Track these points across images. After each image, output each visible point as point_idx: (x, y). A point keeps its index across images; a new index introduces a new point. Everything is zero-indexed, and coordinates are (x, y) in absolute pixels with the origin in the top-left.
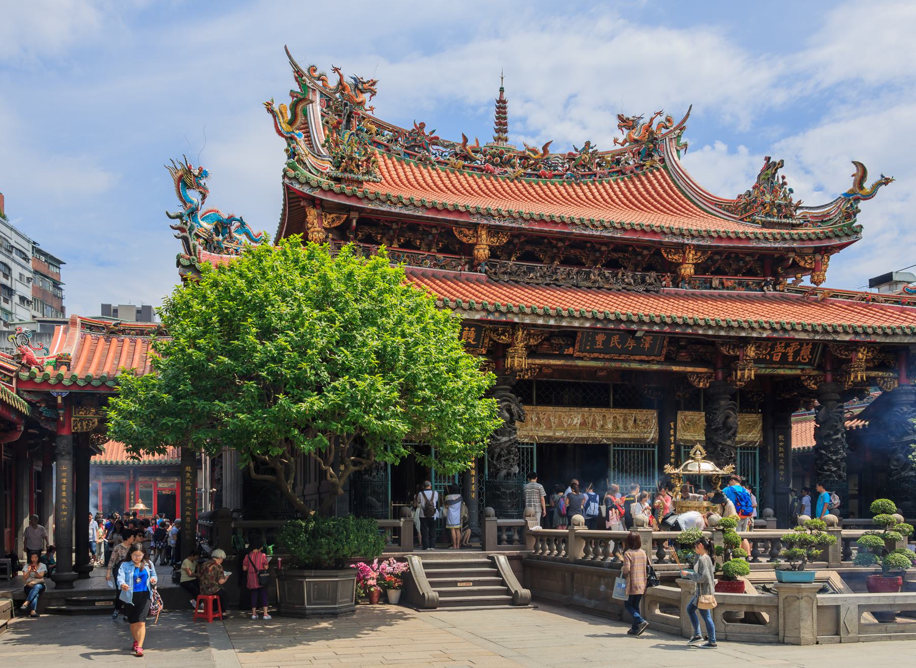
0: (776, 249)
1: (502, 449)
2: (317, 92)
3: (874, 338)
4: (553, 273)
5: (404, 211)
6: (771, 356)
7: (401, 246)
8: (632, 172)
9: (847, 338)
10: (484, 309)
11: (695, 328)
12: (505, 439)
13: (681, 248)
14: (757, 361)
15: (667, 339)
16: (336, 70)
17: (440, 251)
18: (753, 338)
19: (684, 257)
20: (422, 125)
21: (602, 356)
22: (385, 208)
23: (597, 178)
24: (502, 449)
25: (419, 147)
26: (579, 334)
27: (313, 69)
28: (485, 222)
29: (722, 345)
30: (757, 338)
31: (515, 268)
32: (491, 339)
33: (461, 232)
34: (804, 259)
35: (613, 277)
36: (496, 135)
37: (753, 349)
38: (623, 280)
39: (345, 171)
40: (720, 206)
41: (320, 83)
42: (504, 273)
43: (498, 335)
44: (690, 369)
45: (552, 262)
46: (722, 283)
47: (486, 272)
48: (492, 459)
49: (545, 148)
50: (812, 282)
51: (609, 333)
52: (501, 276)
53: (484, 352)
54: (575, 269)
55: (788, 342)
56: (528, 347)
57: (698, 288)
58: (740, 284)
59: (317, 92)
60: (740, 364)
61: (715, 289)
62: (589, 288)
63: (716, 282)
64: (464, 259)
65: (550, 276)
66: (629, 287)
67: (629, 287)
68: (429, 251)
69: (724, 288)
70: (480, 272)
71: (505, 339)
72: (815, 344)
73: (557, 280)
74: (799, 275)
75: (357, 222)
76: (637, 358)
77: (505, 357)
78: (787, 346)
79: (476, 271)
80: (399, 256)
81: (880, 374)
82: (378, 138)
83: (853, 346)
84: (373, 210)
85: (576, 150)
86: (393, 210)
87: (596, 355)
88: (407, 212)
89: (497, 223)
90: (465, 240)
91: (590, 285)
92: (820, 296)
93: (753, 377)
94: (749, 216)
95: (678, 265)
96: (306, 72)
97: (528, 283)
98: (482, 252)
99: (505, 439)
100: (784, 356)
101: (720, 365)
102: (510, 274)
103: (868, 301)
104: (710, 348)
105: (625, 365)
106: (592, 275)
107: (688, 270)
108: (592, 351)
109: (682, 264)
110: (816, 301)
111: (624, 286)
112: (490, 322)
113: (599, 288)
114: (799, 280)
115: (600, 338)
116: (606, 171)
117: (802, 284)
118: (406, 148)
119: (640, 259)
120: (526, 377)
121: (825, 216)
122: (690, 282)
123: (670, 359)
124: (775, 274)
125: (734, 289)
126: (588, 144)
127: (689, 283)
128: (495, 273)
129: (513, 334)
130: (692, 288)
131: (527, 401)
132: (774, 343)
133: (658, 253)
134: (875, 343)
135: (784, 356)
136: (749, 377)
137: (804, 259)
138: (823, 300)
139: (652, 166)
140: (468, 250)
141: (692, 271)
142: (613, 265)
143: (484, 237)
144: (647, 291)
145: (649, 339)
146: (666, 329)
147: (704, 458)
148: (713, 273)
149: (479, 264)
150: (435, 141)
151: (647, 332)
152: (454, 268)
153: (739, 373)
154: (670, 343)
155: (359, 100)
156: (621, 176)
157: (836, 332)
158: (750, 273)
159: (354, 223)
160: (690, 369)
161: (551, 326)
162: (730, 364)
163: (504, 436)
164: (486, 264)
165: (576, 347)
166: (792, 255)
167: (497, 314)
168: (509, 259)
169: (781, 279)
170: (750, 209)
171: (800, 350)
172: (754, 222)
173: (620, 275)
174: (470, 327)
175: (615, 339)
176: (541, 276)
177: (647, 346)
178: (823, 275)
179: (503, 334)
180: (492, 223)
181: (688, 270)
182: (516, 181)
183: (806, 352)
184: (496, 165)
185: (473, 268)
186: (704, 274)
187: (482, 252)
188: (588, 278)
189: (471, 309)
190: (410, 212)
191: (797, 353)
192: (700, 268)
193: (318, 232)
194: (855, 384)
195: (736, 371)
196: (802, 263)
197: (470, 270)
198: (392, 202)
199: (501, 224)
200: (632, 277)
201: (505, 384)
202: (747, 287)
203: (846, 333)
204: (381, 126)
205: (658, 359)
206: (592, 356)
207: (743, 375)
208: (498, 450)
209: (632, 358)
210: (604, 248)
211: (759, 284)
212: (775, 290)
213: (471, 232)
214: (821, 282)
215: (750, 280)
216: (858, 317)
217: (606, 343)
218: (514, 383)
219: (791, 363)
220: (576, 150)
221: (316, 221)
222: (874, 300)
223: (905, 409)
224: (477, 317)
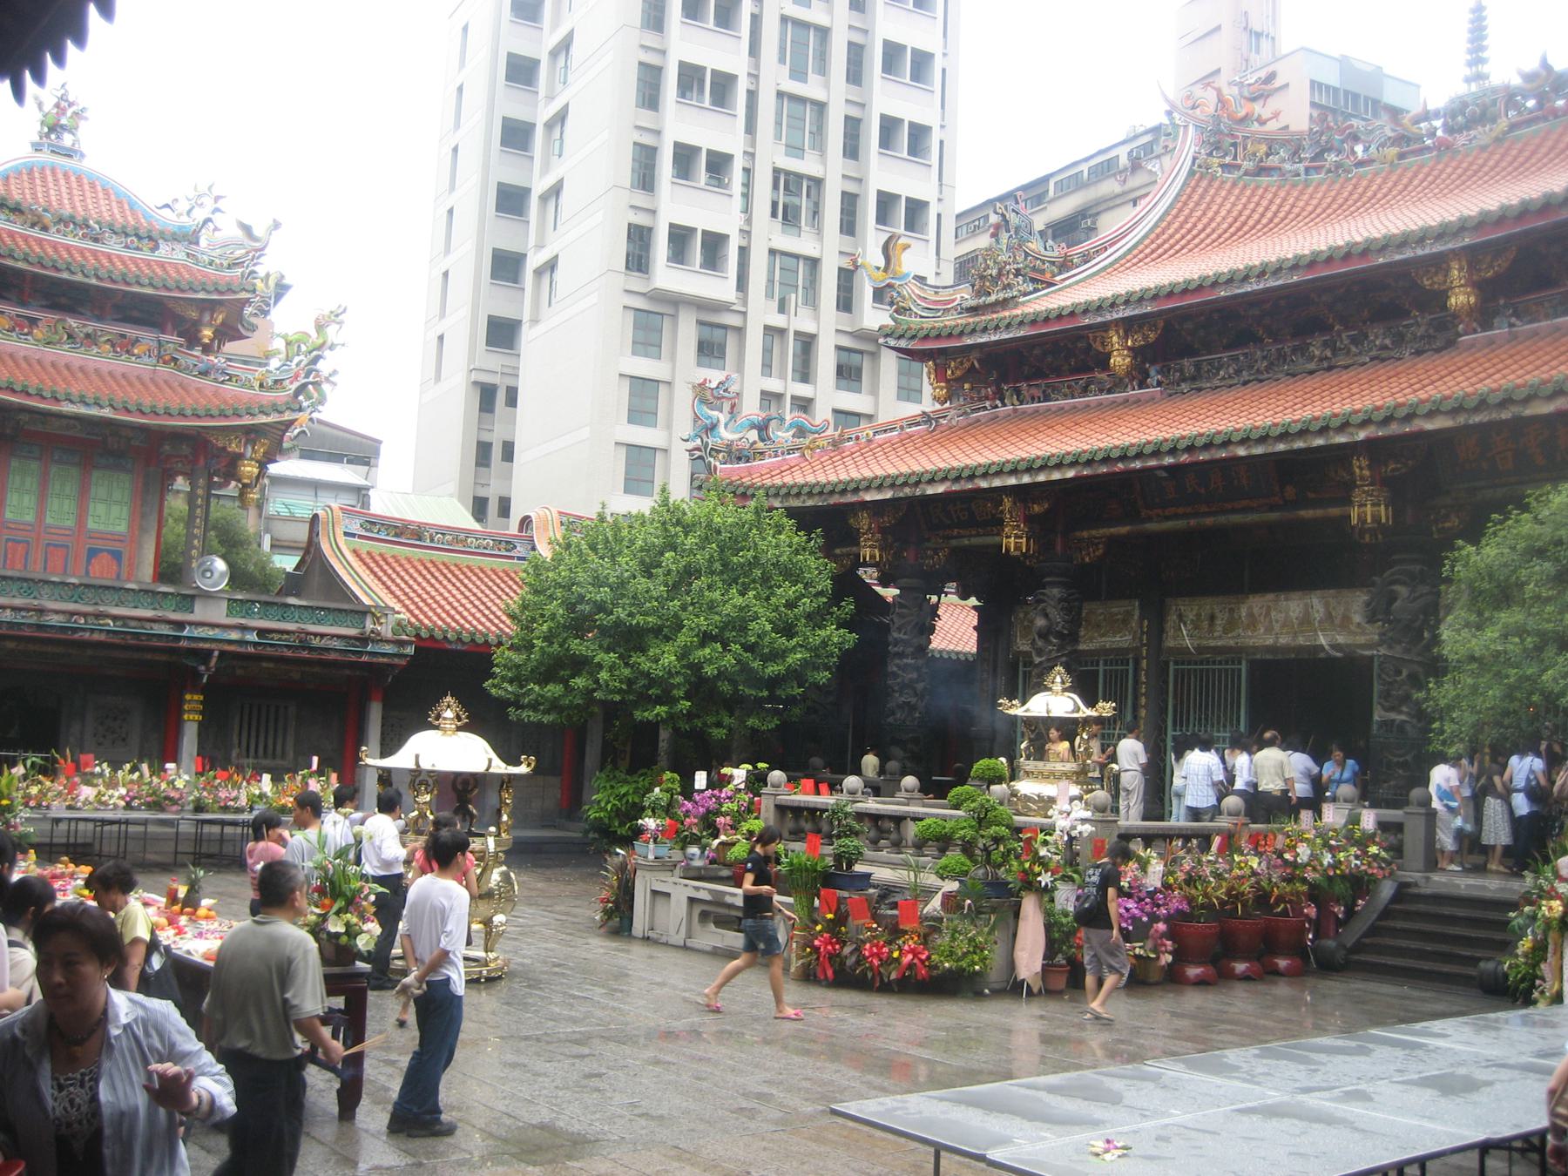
2: (1191, 129)
13: (1438, 263)
21: (1181, 510)
25: (1329, 150)
39: (978, 294)
42: (1184, 380)
47: (1159, 384)
57: (1547, 317)
59: (1191, 129)
66: (1385, 354)
73: (1258, 371)
82: (1273, 161)
91: (1312, 366)
95: (1443, 296)
98: (1120, 361)
102: (1193, 379)
111: (1374, 353)
118: (1313, 160)
140: (1103, 361)
143: (1115, 339)
155: (1242, 113)
181: (1460, 299)
184: (1460, 131)
187: (1120, 361)
204: (1272, 144)
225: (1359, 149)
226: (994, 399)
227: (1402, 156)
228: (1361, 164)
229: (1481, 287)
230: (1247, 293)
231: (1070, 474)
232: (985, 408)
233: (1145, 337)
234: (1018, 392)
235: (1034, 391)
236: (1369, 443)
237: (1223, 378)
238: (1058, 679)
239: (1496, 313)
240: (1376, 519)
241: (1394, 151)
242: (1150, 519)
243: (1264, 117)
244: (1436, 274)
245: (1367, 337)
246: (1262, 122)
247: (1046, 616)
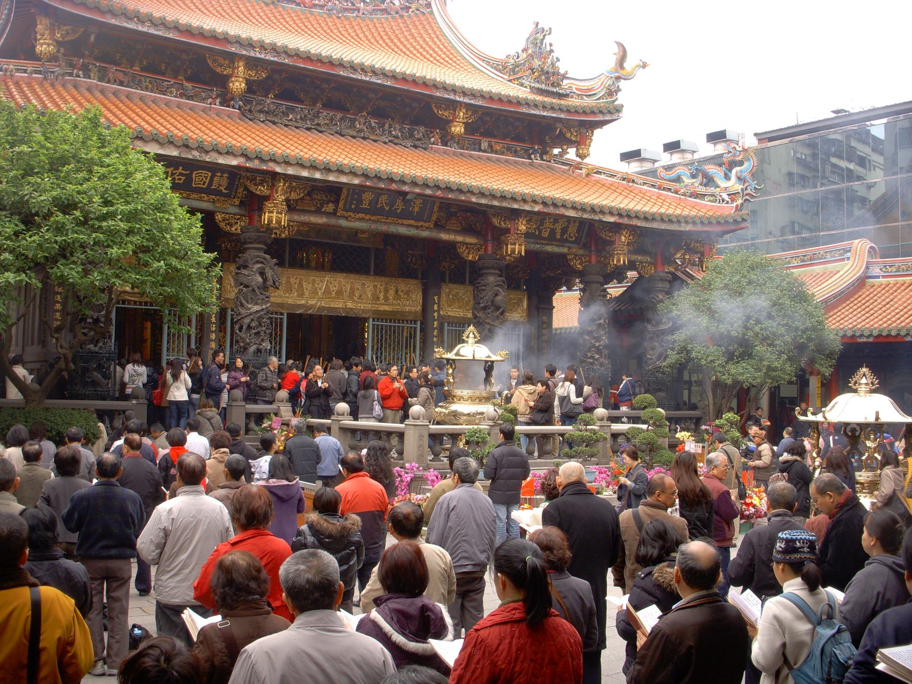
0: (544, 116)
1: (252, 320)
3: (635, 222)
4: (314, 116)
5: (152, 31)
6: (540, 232)
7: (143, 69)
8: (397, 13)
9: (612, 219)
10: (243, 155)
12: (256, 308)
13: (453, 105)
14: (527, 235)
15: (437, 204)
17: (188, 79)
18: (524, 211)
19: (454, 114)
21: (368, 217)
22: (131, 26)
23: (360, 14)
24: (252, 320)
26: (345, 191)
28: (244, 52)
29: (494, 215)
30: (528, 212)
31: (273, 107)
32: (246, 189)
33: (215, 61)
34: (570, 131)
35: (379, 128)
37: (524, 222)
38: (390, 132)
40: (488, 63)
42: (261, 111)
43: (255, 185)
44: (459, 238)
45: (314, 104)
46: (490, 146)
47: (239, 109)
48: (240, 330)
50: (577, 156)
51: (378, 192)
52: (257, 115)
53: (237, 203)
54: (339, 115)
55: (557, 218)
56: (287, 201)
57: (467, 149)
58: (509, 149)
60: (511, 238)
61: (484, 151)
62: (354, 137)
63: (484, 145)
64: (216, 91)
65: (312, 120)
66: (396, 141)
67: (396, 141)
68: (175, 78)
69: (492, 152)
70: (233, 107)
71: (262, 190)
72: (582, 222)
73: (318, 125)
74: (565, 147)
75: (96, 38)
76: (405, 222)
77: (261, 210)
78: (556, 221)
79: (228, 106)
80: (140, 81)
81: (639, 258)
83: (616, 228)
84: (116, 26)
86: (140, 28)
88: (156, 33)
89: (258, 55)
90: (218, 70)
91: (355, 134)
92: (584, 171)
93: (523, 254)
94: (518, 79)
95: (448, 122)
97: (286, 126)
98: (238, 85)
99: (256, 308)
100: (553, 232)
101: (490, 238)
102: (267, 113)
103: (629, 182)
104: (480, 217)
105: (393, 229)
106: (357, 123)
107: (458, 129)
108: (358, 210)
109: (452, 121)
110: (580, 175)
112: (248, 169)
113: (364, 138)
114: (564, 152)
115: (367, 197)
116: (370, 8)
117: (567, 156)
119: (411, 111)
120: (283, 236)
121: (590, 90)
122: (460, 141)
123: (438, 226)
124: (542, 142)
125: (503, 154)
127: (458, 143)
128: (250, 111)
129: (273, 185)
130: (461, 148)
131: (281, 264)
132: (547, 219)
133: (428, 106)
134: (636, 226)
135: (553, 232)
136: (520, 252)
137: (570, 131)
138: (588, 175)
139: (418, 10)
140: (222, 82)
141: (463, 130)
142: (380, 114)
143: (241, 69)
144: (415, 147)
145: (418, 202)
146: (439, 193)
147: (476, 342)
148: (484, 135)
149: (232, 99)
151: (419, 194)
152: (203, 100)
153: (509, 246)
154: (440, 208)
156: (386, 16)
157: (602, 212)
158: (518, 138)
159: (92, 38)
160: (459, 238)
161: (316, 180)
162: (500, 236)
163: (257, 304)
164: (241, 100)
165: (341, 205)
166: (559, 125)
167: (257, 162)
168: (266, 96)
169: (548, 149)
170: (518, 72)
171: (567, 227)
172: (522, 85)
173: (387, 126)
174: (222, 173)
175: (383, 199)
176: (301, 119)
177: (416, 209)
178: (588, 149)
179: (261, 184)
180: (252, 54)
181: (458, 129)
182: (272, 7)
183: (572, 230)
185: (225, 102)
186: (473, 135)
187: (238, 85)
188: (352, 126)
189: (228, 153)
190: (160, 33)
192: (470, 128)
193: (49, 45)
194: (617, 267)
195: (507, 245)
196: (568, 135)
197: (221, 104)
198: (139, 20)
199: (262, 56)
200: (400, 131)
201: (259, 243)
202: (516, 153)
203: (611, 214)
205: (427, 225)
206: (357, 216)
207: (513, 251)
208: (247, 321)
209: (400, 221)
210: (372, 96)
211: (526, 151)
212: (542, 159)
213: (227, 62)
214: (585, 157)
215: (518, 146)
216: (620, 198)
218: (269, 241)
219: (556, 240)
221: (47, 32)
222: (633, 181)
223: (661, 297)
224: (234, 162)
226: (80, 69)
230: (357, 80)
231: (356, 181)
232: (71, 74)
235: (120, 76)
236: (538, 213)
237: (291, 120)
238: (471, 335)
242: (343, 217)
244: (445, 110)
245: (383, 126)
247: (262, 274)
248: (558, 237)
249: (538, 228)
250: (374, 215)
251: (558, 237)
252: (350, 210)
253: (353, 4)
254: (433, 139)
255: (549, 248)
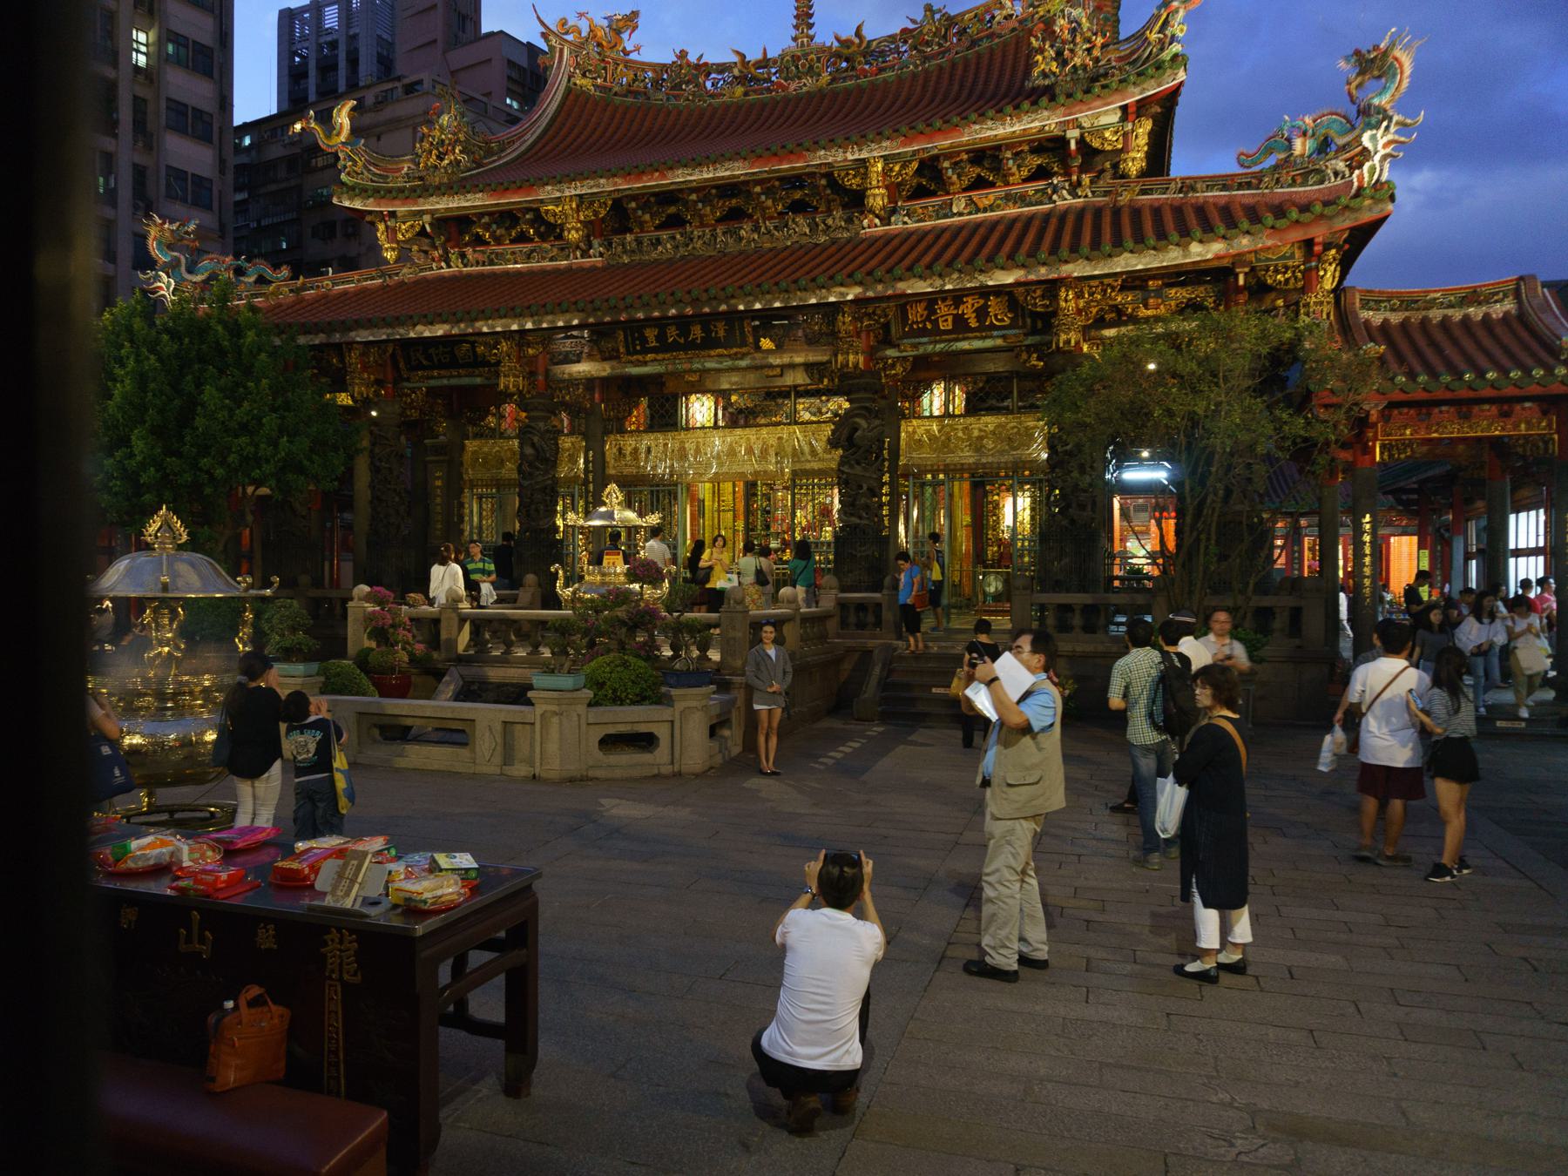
11: (714, 303)
16: (581, 15)
20: (683, 54)
21: (660, 356)
25: (687, 83)
27: (564, 22)
36: (793, 33)
41: (570, 38)
47: (601, 255)
49: (858, 33)
58: (1008, 198)
61: (961, 214)
63: (959, 205)
69: (978, 211)
76: (712, 353)
85: (913, 21)
87: (650, 356)
96: (554, 28)
108: (646, 351)
115: (651, 334)
118: (672, 88)
126: (929, 8)
150: (704, 69)
177: (722, 333)
191: (982, 313)
205: (744, 350)
217: (661, 337)
220: (913, 21)
225: (709, 84)
227: (746, 94)
228: (712, 96)
229: (894, 190)
233: (596, 213)
234: (463, 256)
239: (894, 211)
240: (856, 366)
241: (739, 90)
243: (629, 49)
246: (627, 53)
248: (973, 324)
249: (928, 319)
250: (666, 351)
251: (973, 324)
252: (636, 352)
253: (940, 45)
254: (866, 222)
255: (964, 345)
